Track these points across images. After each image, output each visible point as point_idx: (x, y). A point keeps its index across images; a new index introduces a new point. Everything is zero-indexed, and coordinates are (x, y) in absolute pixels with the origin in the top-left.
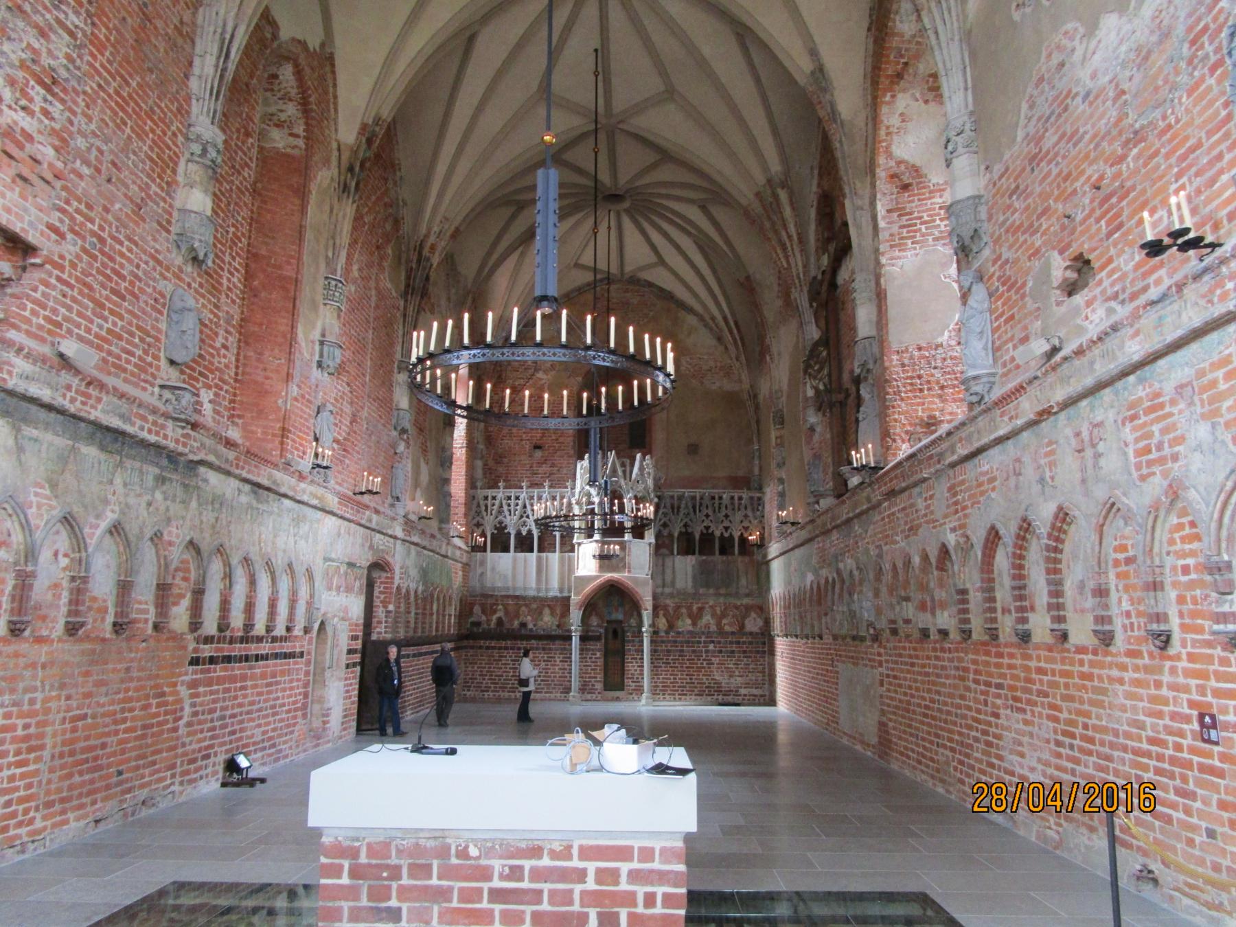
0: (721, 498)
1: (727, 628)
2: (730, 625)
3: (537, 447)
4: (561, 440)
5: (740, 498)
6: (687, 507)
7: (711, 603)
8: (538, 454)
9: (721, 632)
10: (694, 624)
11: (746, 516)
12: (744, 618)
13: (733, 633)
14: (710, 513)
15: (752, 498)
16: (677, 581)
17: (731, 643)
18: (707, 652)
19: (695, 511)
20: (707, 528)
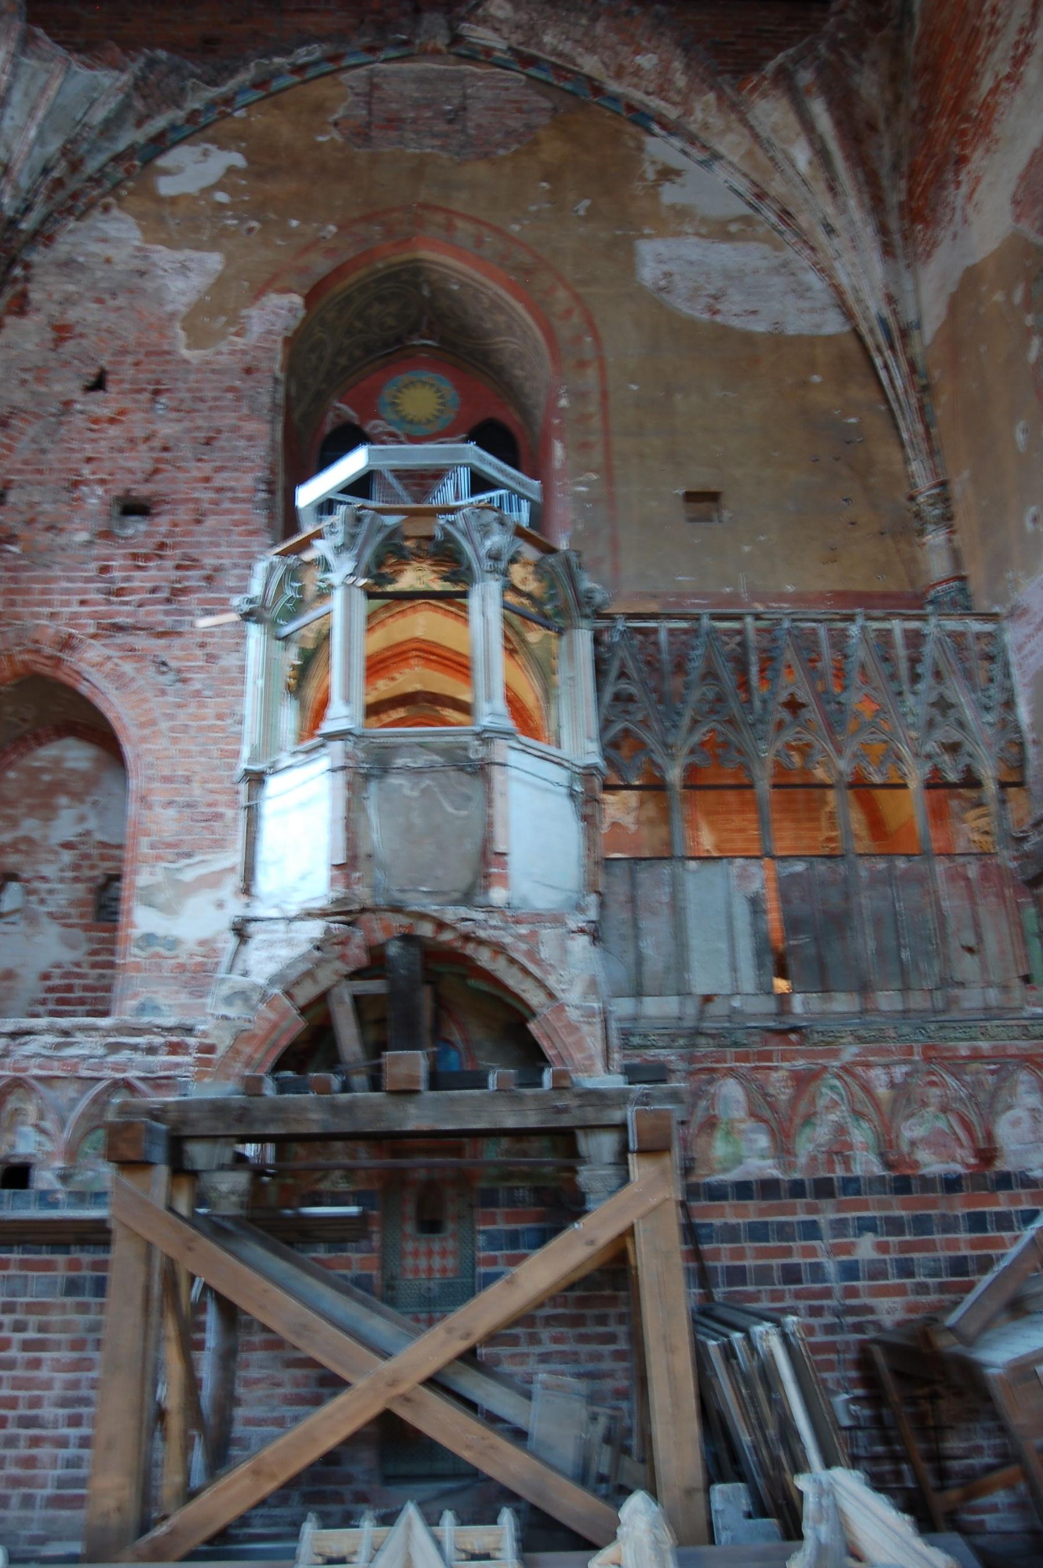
0: (839, 640)
1: (932, 1164)
2: (935, 1142)
3: (134, 508)
4: (219, 481)
5: (915, 639)
6: (710, 675)
7: (850, 1052)
8: (136, 527)
9: (903, 1182)
10: (783, 1146)
11: (943, 705)
12: (990, 1106)
13: (952, 1184)
14: (803, 695)
15: (958, 637)
16: (695, 959)
17: (949, 1225)
18: (850, 1271)
19: (744, 685)
20: (805, 750)
